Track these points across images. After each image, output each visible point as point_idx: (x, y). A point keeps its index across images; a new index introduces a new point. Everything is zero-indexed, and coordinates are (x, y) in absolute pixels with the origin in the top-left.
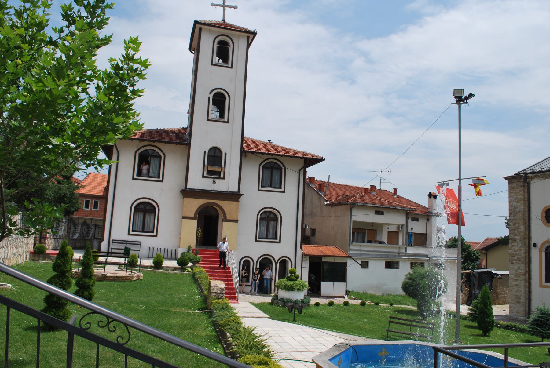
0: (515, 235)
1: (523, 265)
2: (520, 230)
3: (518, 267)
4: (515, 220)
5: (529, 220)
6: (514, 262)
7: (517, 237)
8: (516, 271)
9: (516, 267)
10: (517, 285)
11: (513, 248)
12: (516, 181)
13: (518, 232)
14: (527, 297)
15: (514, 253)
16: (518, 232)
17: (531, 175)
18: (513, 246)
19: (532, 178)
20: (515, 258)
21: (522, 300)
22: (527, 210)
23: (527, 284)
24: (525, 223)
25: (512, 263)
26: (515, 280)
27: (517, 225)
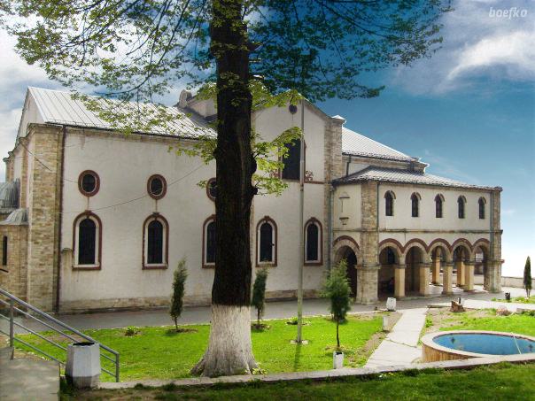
0: (42, 205)
1: (53, 244)
2: (50, 199)
3: (46, 248)
4: (43, 184)
5: (62, 186)
6: (40, 241)
7: (45, 208)
8: (42, 253)
9: (42, 248)
10: (43, 271)
11: (39, 222)
12: (49, 131)
13: (47, 201)
14: (56, 284)
15: (39, 229)
16: (47, 201)
17: (70, 128)
18: (38, 219)
19: (69, 132)
20: (42, 236)
21: (51, 290)
22: (59, 172)
23: (56, 268)
24: (57, 190)
25: (38, 243)
26: (41, 265)
27: (46, 192)
